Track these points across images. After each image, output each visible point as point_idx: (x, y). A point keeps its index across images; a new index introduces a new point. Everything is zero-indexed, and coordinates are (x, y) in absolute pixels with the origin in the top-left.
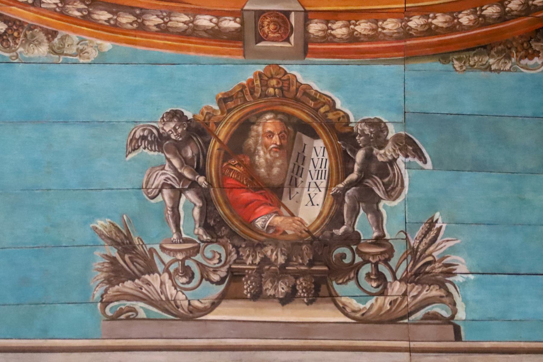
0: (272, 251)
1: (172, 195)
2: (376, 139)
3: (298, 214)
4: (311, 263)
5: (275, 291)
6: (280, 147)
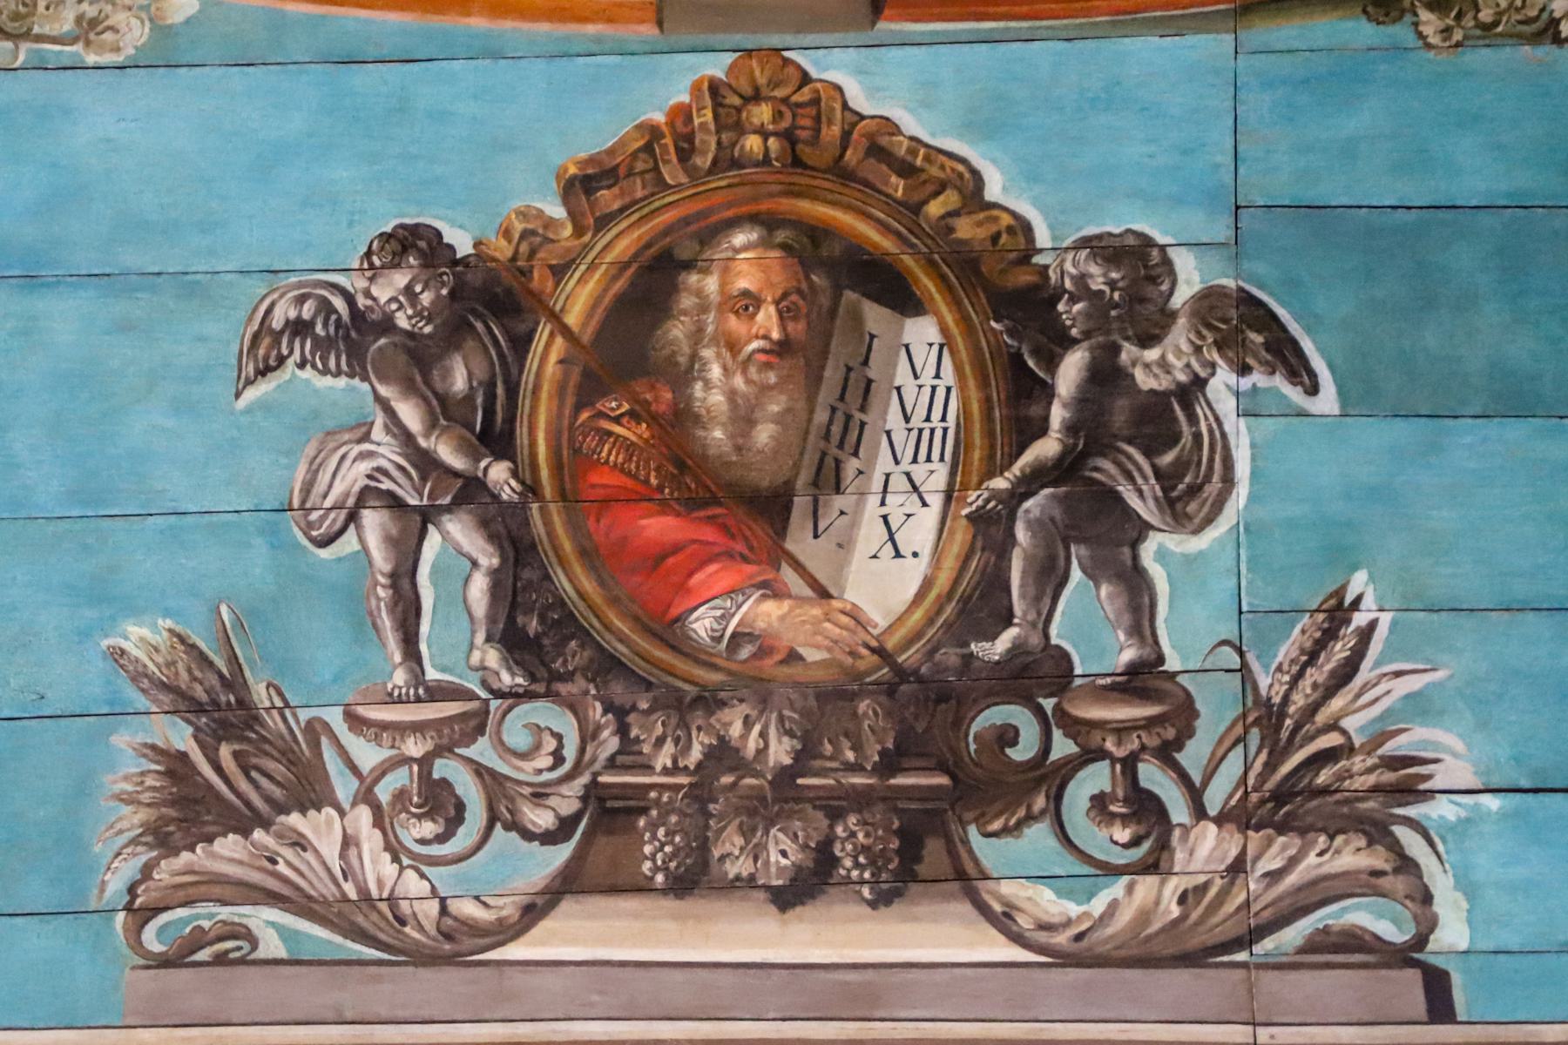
0: (748, 723)
1: (394, 532)
2: (1131, 308)
3: (842, 590)
4: (890, 764)
5: (756, 859)
6: (783, 348)
